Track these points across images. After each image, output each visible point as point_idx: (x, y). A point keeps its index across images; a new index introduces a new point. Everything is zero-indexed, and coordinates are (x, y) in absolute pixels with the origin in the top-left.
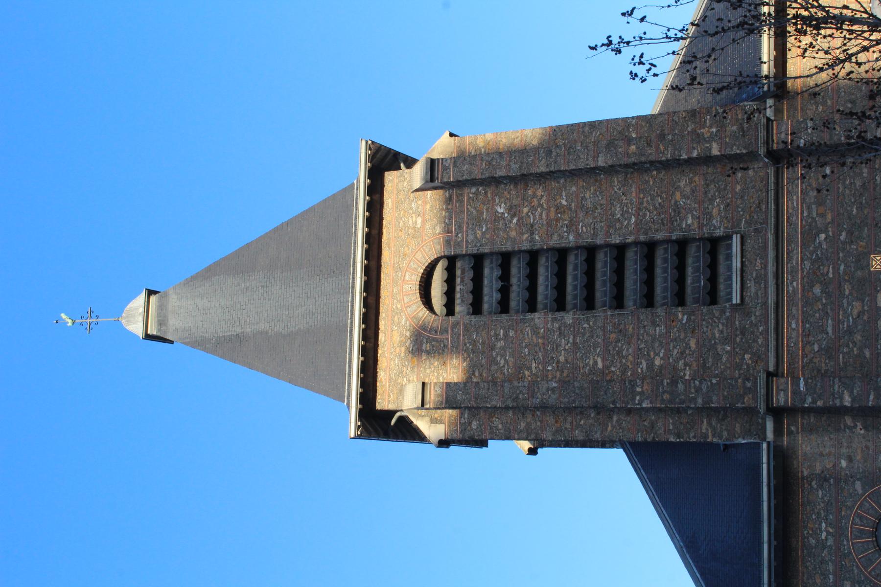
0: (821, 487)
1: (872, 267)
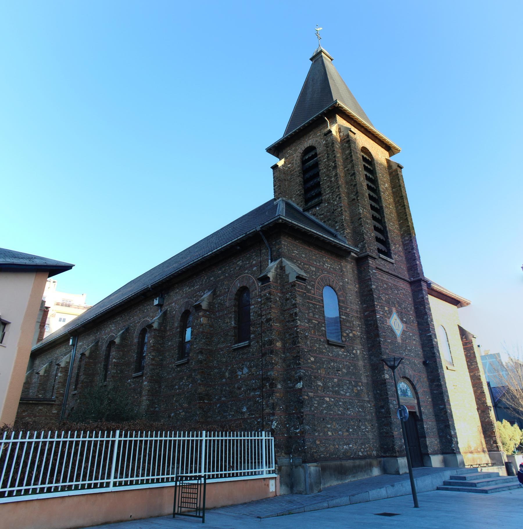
0: (339, 268)
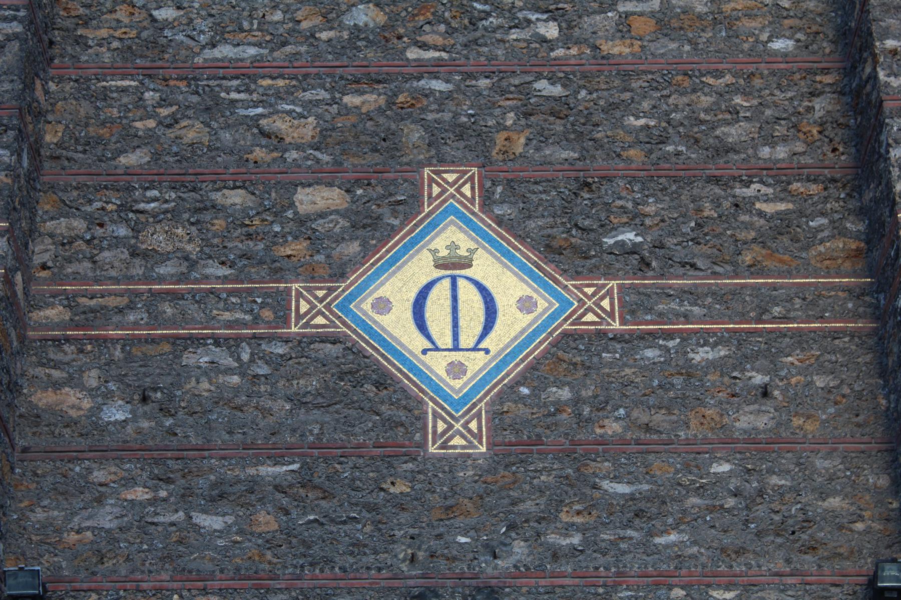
1: (437, 173)
